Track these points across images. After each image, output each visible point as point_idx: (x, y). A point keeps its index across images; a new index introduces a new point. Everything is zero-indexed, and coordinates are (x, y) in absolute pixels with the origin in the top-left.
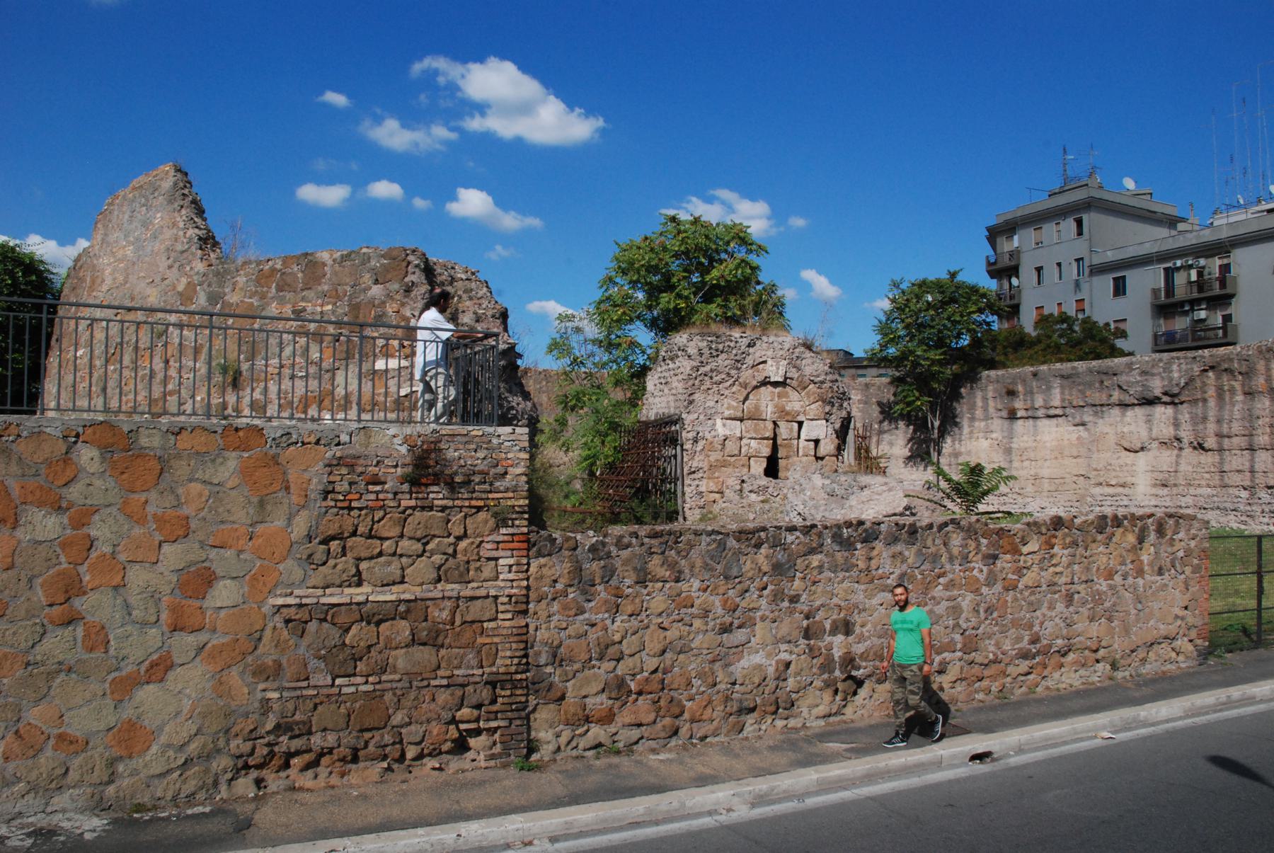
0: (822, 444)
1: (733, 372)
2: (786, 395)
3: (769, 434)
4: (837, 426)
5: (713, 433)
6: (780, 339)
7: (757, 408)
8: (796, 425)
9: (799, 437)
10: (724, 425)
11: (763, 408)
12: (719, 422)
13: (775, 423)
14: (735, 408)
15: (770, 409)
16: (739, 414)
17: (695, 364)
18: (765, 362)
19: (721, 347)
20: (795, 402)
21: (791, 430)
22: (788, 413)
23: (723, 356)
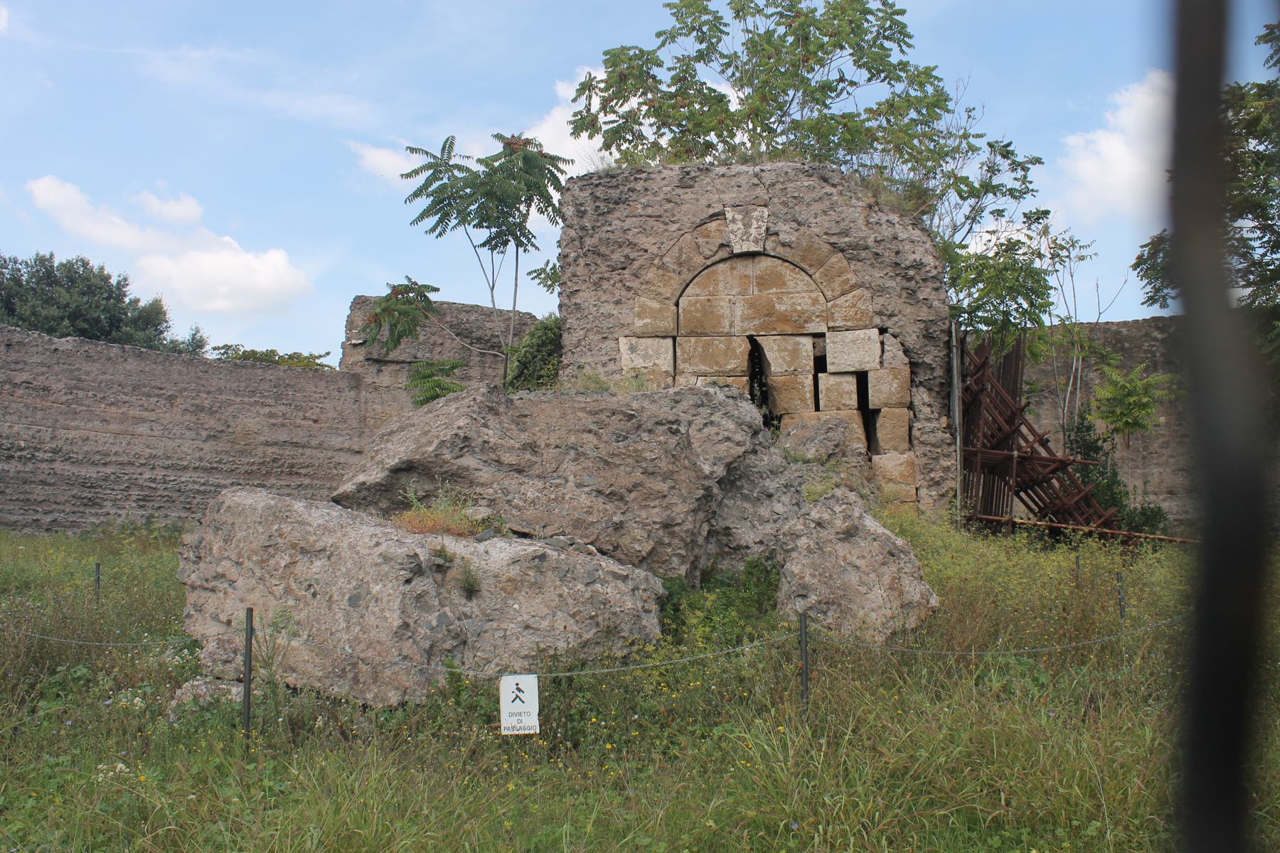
0: (870, 375)
1: (644, 241)
2: (779, 281)
3: (738, 359)
4: (912, 340)
5: (611, 367)
6: (757, 169)
7: (708, 308)
8: (807, 343)
9: (820, 364)
10: (633, 349)
11: (723, 307)
12: (624, 344)
13: (751, 339)
14: (655, 314)
15: (738, 312)
16: (667, 324)
17: (572, 233)
18: (719, 216)
19: (615, 194)
20: (798, 294)
21: (795, 353)
22: (785, 318)
23: (622, 211)
